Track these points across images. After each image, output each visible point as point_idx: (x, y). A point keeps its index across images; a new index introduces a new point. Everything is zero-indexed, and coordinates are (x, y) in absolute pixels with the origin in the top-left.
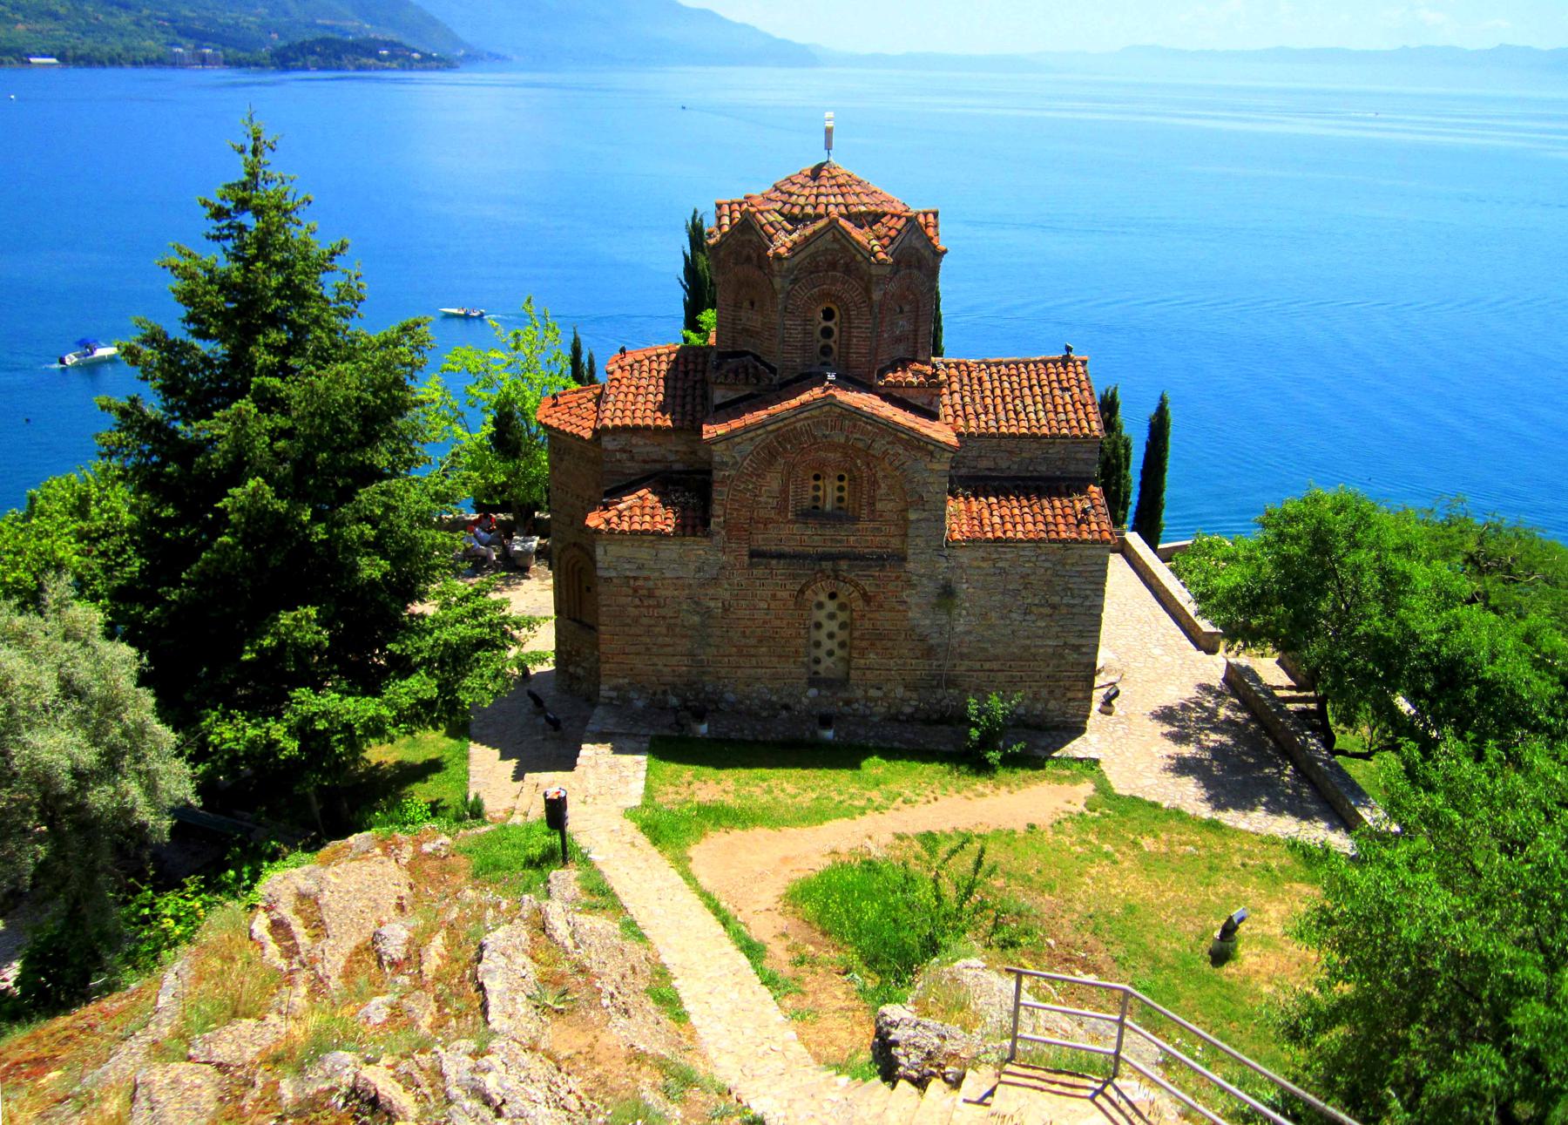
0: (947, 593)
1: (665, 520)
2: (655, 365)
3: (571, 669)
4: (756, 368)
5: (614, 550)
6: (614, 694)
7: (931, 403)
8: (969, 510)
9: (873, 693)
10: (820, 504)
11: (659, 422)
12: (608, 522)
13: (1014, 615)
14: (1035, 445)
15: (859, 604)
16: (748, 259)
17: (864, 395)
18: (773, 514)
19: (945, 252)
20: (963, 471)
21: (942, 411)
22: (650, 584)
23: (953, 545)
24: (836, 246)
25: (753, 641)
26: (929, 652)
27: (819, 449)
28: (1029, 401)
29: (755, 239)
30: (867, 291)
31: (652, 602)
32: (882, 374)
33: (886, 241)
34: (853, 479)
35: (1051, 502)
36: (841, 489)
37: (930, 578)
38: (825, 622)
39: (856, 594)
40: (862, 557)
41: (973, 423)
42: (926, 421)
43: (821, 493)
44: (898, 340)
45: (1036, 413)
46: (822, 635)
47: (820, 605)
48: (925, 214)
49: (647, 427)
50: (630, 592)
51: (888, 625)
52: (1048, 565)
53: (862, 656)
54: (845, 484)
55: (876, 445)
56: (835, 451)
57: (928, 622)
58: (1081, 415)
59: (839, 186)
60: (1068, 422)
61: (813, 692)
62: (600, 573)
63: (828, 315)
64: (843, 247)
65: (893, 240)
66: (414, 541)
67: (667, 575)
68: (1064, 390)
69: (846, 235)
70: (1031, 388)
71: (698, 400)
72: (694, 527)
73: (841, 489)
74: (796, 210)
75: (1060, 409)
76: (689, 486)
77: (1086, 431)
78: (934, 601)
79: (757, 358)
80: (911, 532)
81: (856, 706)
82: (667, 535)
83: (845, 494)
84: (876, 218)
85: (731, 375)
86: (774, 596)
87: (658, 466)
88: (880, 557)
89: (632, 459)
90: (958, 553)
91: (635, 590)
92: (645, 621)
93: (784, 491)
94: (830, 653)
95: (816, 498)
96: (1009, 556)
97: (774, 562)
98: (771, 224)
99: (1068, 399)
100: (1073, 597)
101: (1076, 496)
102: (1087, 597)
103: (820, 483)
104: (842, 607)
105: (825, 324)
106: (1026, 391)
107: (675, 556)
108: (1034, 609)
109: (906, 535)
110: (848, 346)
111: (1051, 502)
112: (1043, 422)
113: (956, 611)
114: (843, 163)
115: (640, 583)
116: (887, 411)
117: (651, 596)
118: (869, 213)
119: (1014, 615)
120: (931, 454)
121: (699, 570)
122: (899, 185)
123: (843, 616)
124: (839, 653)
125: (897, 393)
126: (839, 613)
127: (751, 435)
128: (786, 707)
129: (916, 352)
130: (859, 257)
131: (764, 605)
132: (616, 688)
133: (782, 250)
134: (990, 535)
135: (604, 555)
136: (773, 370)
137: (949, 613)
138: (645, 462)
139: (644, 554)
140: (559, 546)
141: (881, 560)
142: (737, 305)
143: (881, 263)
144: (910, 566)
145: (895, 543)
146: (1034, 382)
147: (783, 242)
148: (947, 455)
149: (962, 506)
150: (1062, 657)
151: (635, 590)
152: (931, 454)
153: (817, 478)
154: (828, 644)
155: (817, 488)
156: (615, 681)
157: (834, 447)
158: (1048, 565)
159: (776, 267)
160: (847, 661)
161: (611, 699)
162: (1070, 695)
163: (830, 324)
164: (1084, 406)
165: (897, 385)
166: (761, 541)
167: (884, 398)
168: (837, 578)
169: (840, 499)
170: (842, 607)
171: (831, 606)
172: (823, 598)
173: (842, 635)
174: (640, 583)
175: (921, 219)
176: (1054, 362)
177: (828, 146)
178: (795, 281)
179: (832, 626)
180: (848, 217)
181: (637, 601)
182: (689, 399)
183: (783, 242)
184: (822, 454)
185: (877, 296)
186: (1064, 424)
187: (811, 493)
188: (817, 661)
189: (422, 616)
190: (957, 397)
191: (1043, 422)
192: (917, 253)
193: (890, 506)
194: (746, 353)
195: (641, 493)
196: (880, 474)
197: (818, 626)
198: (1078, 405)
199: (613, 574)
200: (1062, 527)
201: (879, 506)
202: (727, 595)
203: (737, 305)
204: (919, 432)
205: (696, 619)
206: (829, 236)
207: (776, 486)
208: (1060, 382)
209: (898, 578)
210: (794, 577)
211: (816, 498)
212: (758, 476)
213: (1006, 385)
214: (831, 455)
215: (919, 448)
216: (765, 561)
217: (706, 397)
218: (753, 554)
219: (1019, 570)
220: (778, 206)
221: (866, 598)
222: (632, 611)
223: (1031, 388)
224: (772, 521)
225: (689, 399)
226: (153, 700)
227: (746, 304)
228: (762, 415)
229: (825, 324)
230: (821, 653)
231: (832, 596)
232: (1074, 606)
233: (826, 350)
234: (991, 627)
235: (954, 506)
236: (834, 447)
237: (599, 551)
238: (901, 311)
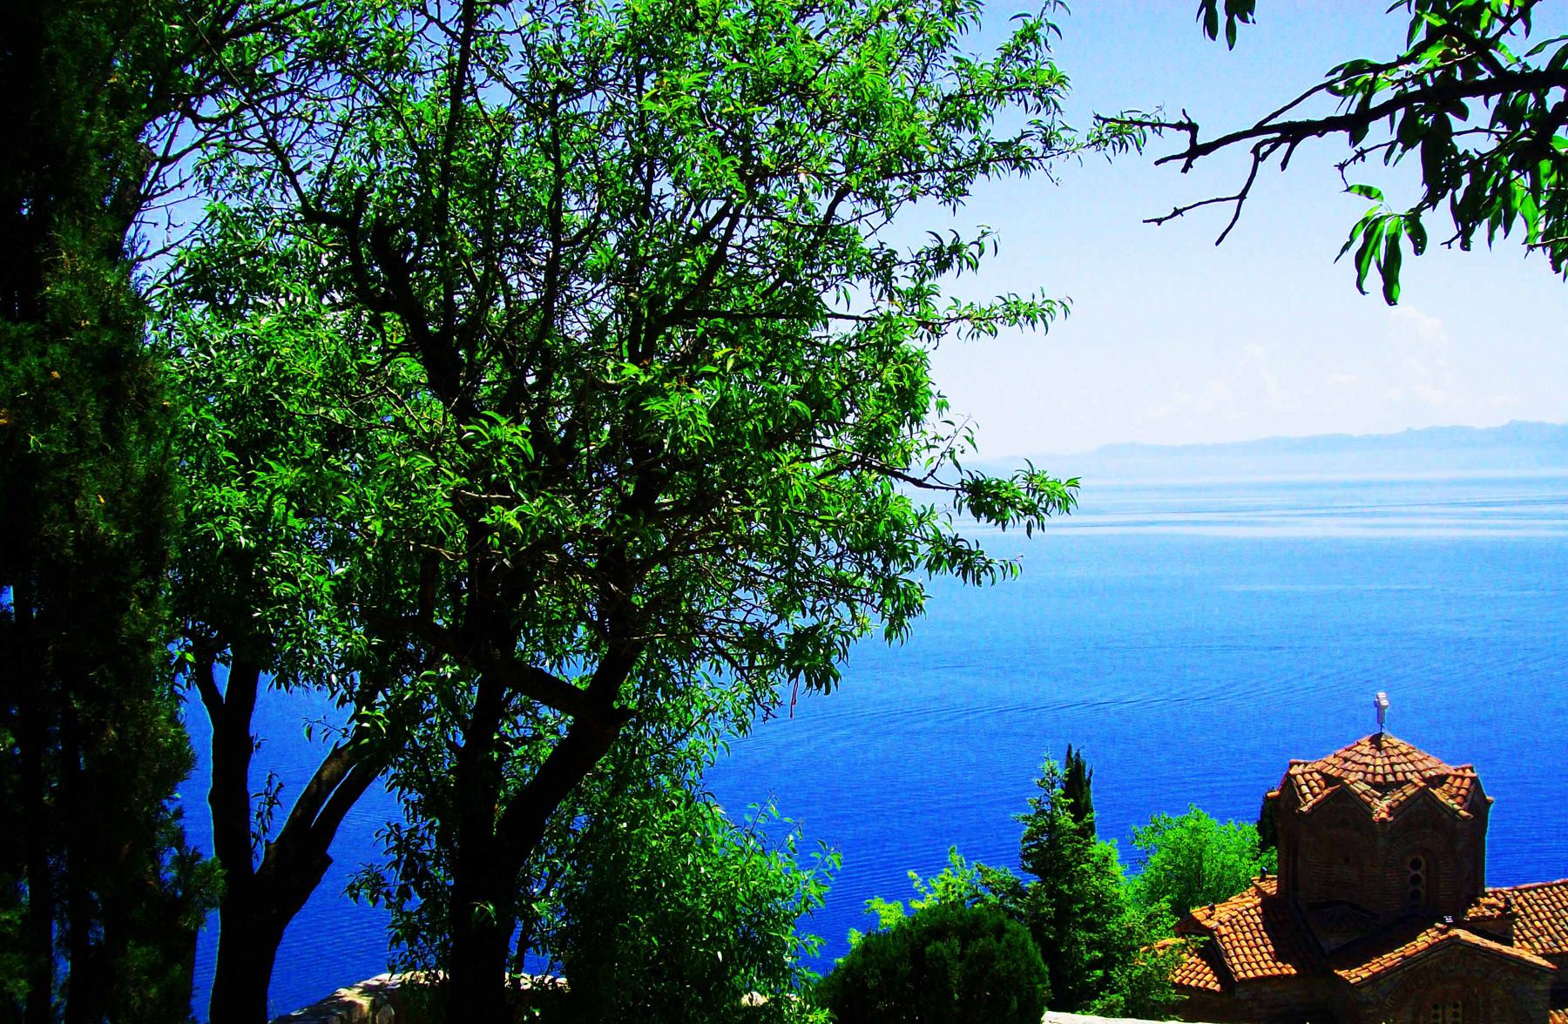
33: (1459, 799)
36: (1455, 1015)
63: (1415, 864)
74: (1379, 779)
103: (1440, 1012)
105: (1414, 873)
120: (1537, 978)
133: (1383, 815)
147: (1381, 808)
153: (1436, 1007)
155: (1436, 1016)
183: (1381, 808)
220: (1360, 775)
228: (1391, 958)
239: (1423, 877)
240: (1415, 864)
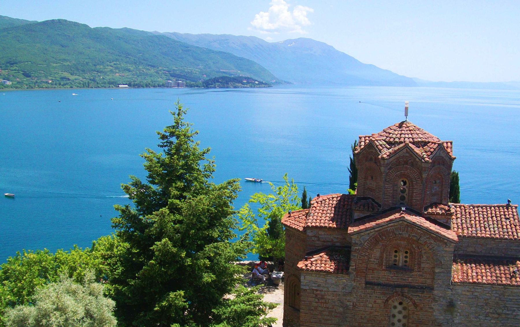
0: (451, 305)
1: (330, 266)
2: (331, 202)
4: (372, 204)
5: (308, 278)
7: (447, 222)
8: (462, 269)
10: (396, 263)
11: (331, 225)
12: (306, 266)
13: (481, 317)
14: (493, 242)
15: (412, 308)
16: (371, 159)
17: (418, 218)
18: (376, 266)
19: (455, 158)
20: (461, 252)
21: (452, 226)
23: (455, 284)
24: (407, 155)
25: (365, 321)
27: (396, 240)
28: (491, 223)
29: (374, 151)
30: (421, 173)
31: (323, 301)
32: (426, 209)
33: (429, 153)
34: (411, 253)
35: (499, 267)
36: (406, 257)
37: (444, 298)
38: (397, 314)
39: (411, 303)
40: (413, 287)
41: (466, 231)
42: (444, 230)
43: (397, 258)
44: (434, 195)
45: (494, 228)
46: (395, 320)
47: (395, 307)
48: (447, 143)
49: (326, 227)
50: (314, 296)
54: (408, 255)
57: (442, 317)
58: (514, 230)
59: (410, 131)
60: (508, 232)
62: (302, 287)
64: (411, 155)
65: (432, 153)
66: (226, 268)
67: (330, 290)
68: (507, 219)
69: (412, 150)
70: (492, 217)
71: (348, 217)
72: (342, 270)
73: (406, 257)
74: (392, 140)
75: (505, 227)
76: (341, 252)
77: (516, 237)
78: (445, 308)
79: (373, 200)
80: (436, 277)
82: (331, 273)
83: (408, 260)
84: (425, 144)
85: (362, 207)
86: (375, 302)
87: (330, 244)
88: (422, 288)
89: (319, 240)
90: (457, 287)
91: (316, 295)
92: (320, 309)
93: (381, 257)
95: (395, 261)
96: (479, 290)
97: (376, 287)
98: (381, 145)
99: (508, 223)
100: (508, 310)
101: (511, 266)
102: (514, 311)
104: (405, 308)
106: (490, 219)
107: (334, 282)
108: (490, 314)
109: (434, 279)
110: (412, 197)
111: (499, 267)
112: (497, 232)
113: (455, 314)
114: (412, 121)
115: (319, 292)
116: (428, 224)
118: (422, 142)
119: (481, 317)
120: (446, 243)
121: (343, 288)
122: (435, 132)
123: (404, 313)
125: (432, 217)
126: (403, 311)
127: (369, 232)
129: (441, 201)
130: (417, 159)
131: (370, 305)
133: (385, 156)
134: (471, 281)
135: (304, 280)
136: (380, 206)
137: (452, 314)
138: (324, 241)
139: (320, 280)
141: (422, 289)
142: (366, 178)
143: (426, 162)
144: (435, 292)
145: (429, 282)
146: (494, 215)
147: (385, 153)
148: (453, 244)
149: (460, 267)
152: (446, 243)
153: (396, 252)
155: (396, 256)
157: (403, 239)
158: (498, 295)
159: (382, 162)
164: (515, 226)
165: (432, 214)
166: (370, 277)
167: (427, 219)
168: (403, 296)
169: (406, 262)
170: (405, 308)
171: (400, 308)
172: (396, 304)
174: (319, 292)
175: (445, 145)
176: (503, 207)
177: (406, 115)
178: (390, 169)
179: (400, 316)
180: (413, 143)
181: (317, 300)
182: (344, 216)
183: (385, 153)
184: (399, 242)
185: (424, 176)
186: (506, 234)
187: (393, 258)
189: (228, 300)
190: (459, 220)
191: (497, 232)
192: (442, 158)
193: (427, 265)
194: (369, 198)
195: (321, 254)
196: (423, 252)
197: (394, 316)
198: (513, 226)
200: (503, 279)
201: (423, 265)
202: (355, 300)
203: (366, 178)
204: (441, 234)
205: (341, 309)
206: (405, 150)
207: (378, 254)
208: (505, 215)
209: (429, 297)
210: (384, 294)
211: (395, 261)
212: (371, 249)
213: (481, 216)
214: (402, 242)
215: (440, 241)
216: (372, 286)
217: (351, 215)
218: (367, 283)
220: (384, 138)
222: (315, 304)
223: (492, 217)
224: (375, 269)
225: (344, 216)
226: (116, 322)
227: (370, 178)
228: (373, 224)
231: (401, 303)
232: (508, 314)
233: (403, 198)
234: (470, 321)
235: (454, 267)
236: (403, 239)
237: (302, 278)
238: (436, 183)
239: (407, 189)
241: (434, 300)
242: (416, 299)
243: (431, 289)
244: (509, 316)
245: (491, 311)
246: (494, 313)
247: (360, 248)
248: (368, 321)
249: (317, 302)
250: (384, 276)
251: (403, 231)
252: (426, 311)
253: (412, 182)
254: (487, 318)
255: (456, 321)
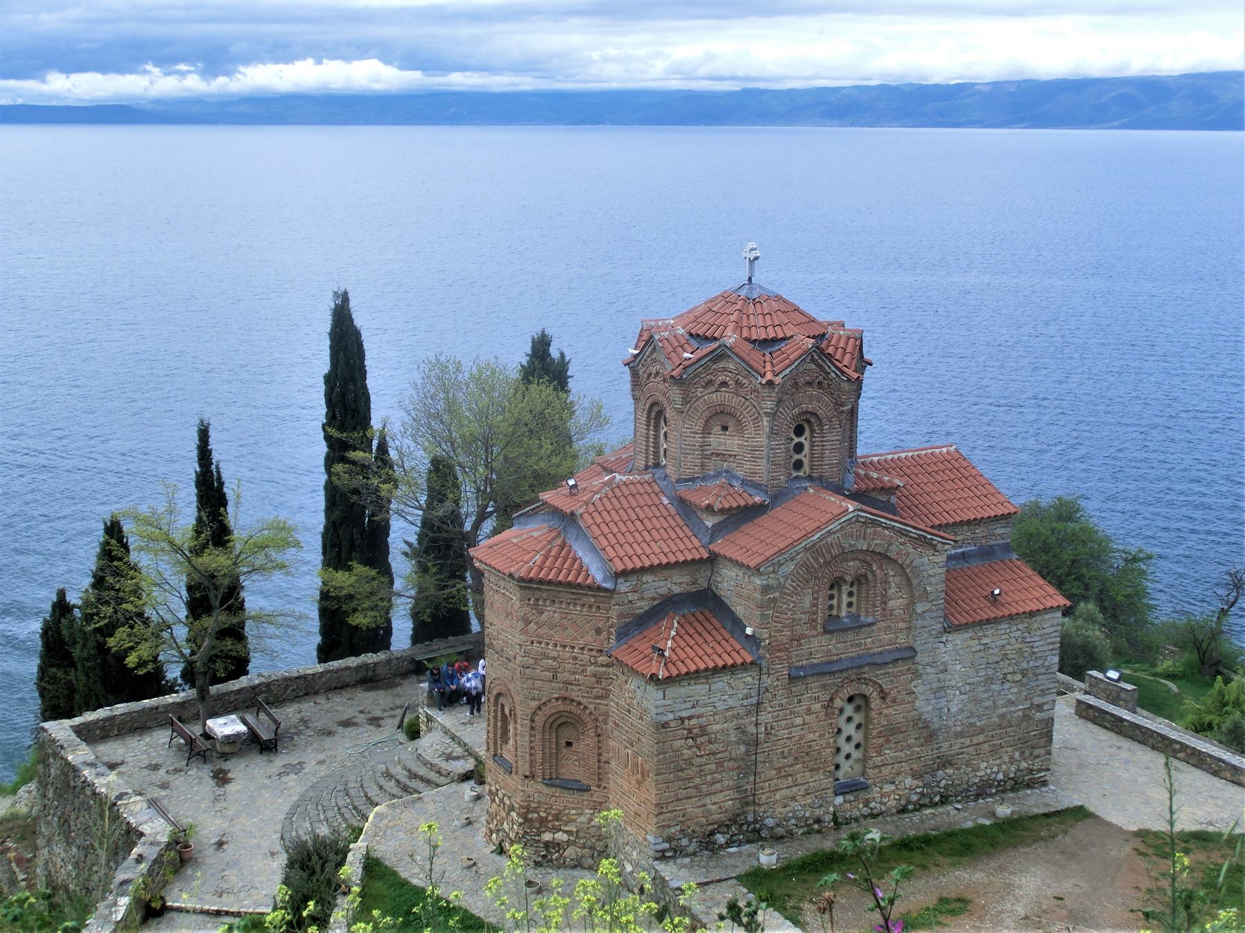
3: (547, 837)
6: (666, 845)
9: (889, 788)
10: (834, 612)
16: (724, 384)
22: (703, 720)
25: (791, 759)
26: (931, 736)
36: (850, 594)
43: (835, 602)
46: (841, 741)
50: (685, 732)
51: (900, 719)
52: (1018, 634)
53: (880, 753)
54: (854, 589)
55: (893, 548)
56: (854, 559)
57: (930, 707)
61: (839, 800)
81: (872, 805)
86: (809, 710)
91: (690, 731)
94: (848, 757)
103: (835, 592)
104: (858, 709)
105: (797, 440)
108: (1009, 677)
110: (822, 458)
117: (703, 730)
119: (995, 687)
123: (858, 718)
124: (856, 754)
128: (818, 821)
131: (799, 721)
132: (669, 840)
140: (534, 704)
142: (706, 431)
144: (918, 658)
150: (1030, 718)
151: (690, 731)
153: (832, 587)
154: (847, 748)
155: (831, 597)
156: (668, 832)
157: (856, 554)
158: (1018, 634)
160: (864, 760)
161: (663, 851)
162: (1036, 752)
163: (802, 439)
169: (850, 605)
170: (858, 709)
171: (849, 710)
173: (858, 737)
174: (693, 722)
181: (690, 742)
188: (837, 767)
197: (839, 731)
199: (671, 716)
201: (891, 604)
203: (706, 431)
207: (807, 601)
210: (824, 687)
211: (831, 607)
214: (851, 563)
219: (998, 644)
221: (883, 696)
222: (687, 753)
224: (802, 636)
227: (717, 429)
229: (797, 440)
230: (841, 759)
231: (851, 699)
233: (798, 465)
240: (799, 431)
241: (917, 675)
242: (885, 684)
243: (909, 654)
244: (1038, 671)
245: (1011, 670)
246: (1014, 673)
247: (777, 595)
248: (796, 759)
249: (690, 748)
250: (820, 647)
251: (857, 538)
252: (903, 702)
253: (821, 424)
254: (1007, 686)
255: (954, 709)
